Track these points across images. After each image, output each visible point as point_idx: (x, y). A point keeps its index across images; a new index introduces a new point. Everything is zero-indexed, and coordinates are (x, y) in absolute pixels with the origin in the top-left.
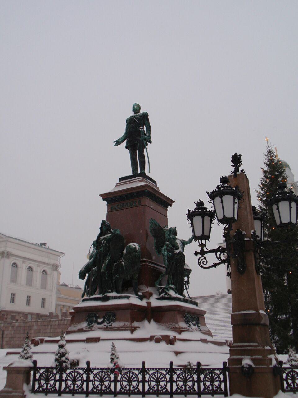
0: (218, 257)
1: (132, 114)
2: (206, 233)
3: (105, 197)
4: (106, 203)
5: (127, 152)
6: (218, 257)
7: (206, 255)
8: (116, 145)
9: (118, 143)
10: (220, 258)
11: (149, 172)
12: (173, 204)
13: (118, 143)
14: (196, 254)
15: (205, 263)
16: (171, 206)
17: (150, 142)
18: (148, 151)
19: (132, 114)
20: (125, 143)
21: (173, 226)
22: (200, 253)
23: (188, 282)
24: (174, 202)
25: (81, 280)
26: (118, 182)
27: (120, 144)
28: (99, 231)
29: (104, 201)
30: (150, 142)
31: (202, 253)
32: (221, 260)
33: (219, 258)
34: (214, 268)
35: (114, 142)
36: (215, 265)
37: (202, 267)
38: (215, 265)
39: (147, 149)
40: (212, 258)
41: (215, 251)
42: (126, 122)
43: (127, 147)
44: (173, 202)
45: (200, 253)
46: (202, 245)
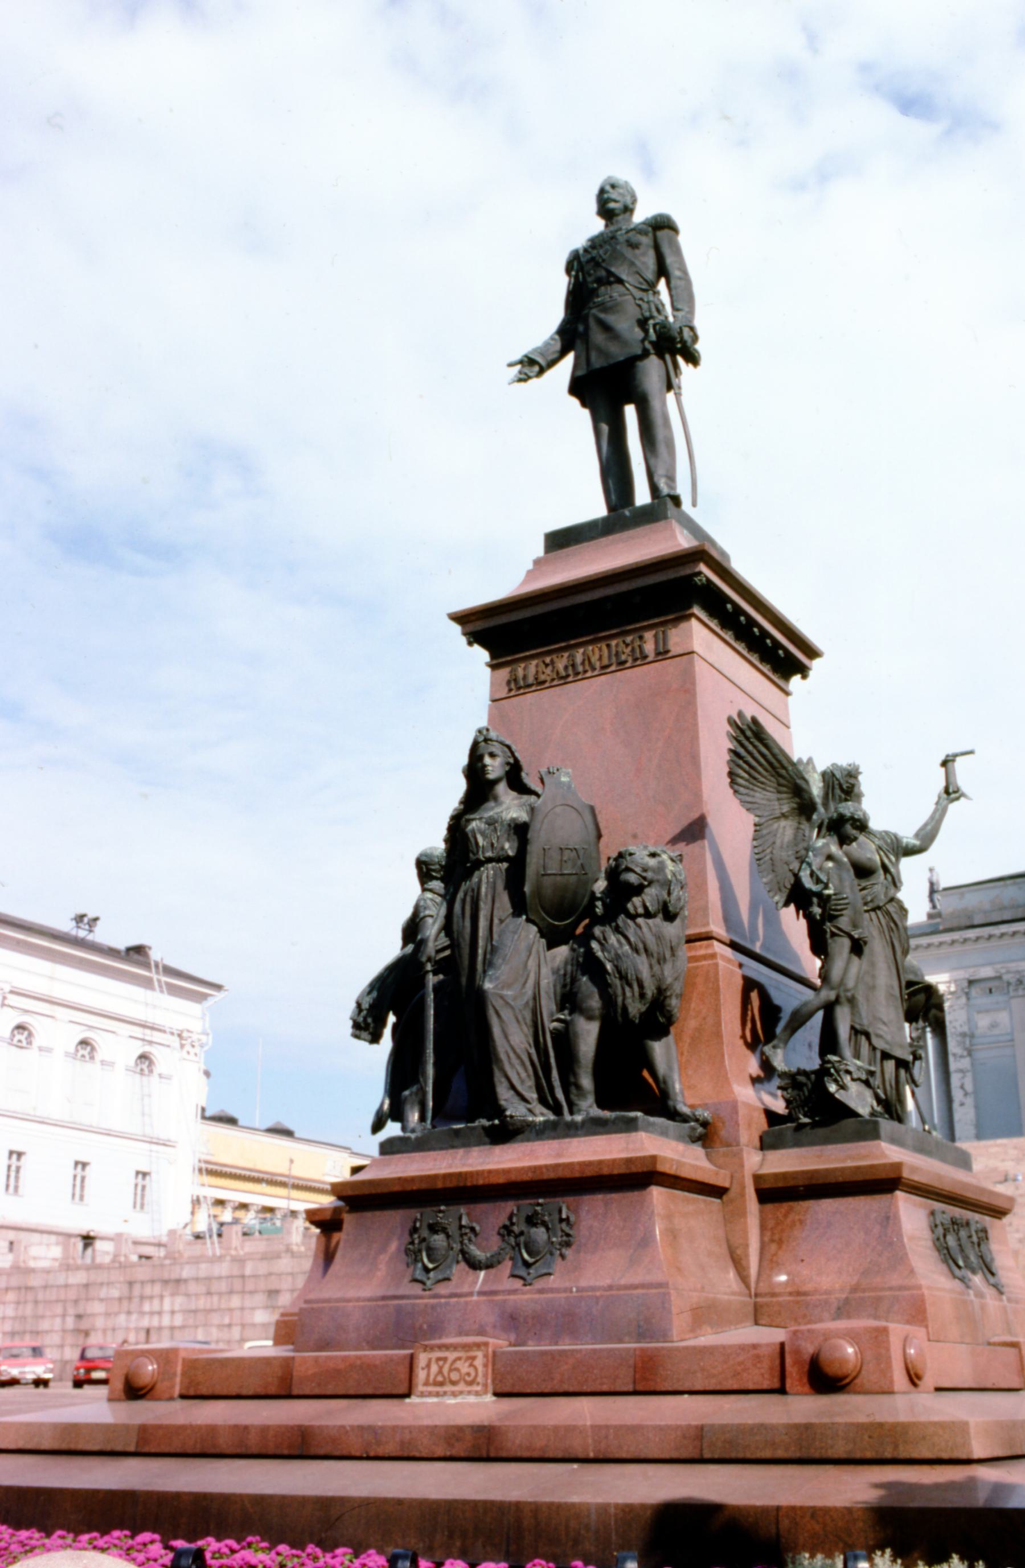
1: (598, 226)
4: (481, 655)
5: (578, 420)
8: (523, 378)
13: (532, 366)
16: (804, 677)
18: (684, 399)
25: (363, 1046)
26: (530, 566)
28: (460, 786)
35: (510, 365)
39: (678, 396)
42: (569, 270)
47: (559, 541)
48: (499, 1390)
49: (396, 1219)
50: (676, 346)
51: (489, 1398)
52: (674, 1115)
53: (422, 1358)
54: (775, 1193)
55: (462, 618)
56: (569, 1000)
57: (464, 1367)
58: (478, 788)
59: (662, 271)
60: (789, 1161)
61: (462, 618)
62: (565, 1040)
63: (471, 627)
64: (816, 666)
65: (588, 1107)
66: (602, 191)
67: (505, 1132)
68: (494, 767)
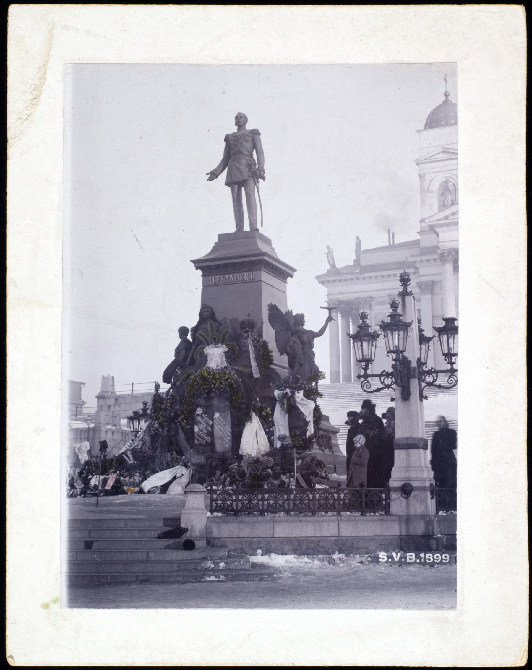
0: (382, 381)
3: (199, 264)
4: (200, 272)
6: (382, 381)
7: (369, 379)
8: (211, 179)
9: (213, 175)
10: (384, 382)
11: (262, 226)
13: (213, 175)
14: (359, 377)
15: (368, 387)
17: (264, 178)
19: (234, 129)
20: (224, 175)
21: (300, 312)
27: (217, 177)
29: (197, 269)
30: (264, 178)
31: (366, 376)
32: (385, 385)
33: (383, 383)
35: (207, 174)
36: (378, 390)
37: (365, 391)
38: (378, 390)
39: (258, 189)
41: (380, 376)
42: (225, 141)
43: (228, 183)
44: (294, 270)
50: (258, 174)
59: (255, 147)
64: (295, 274)
66: (237, 118)
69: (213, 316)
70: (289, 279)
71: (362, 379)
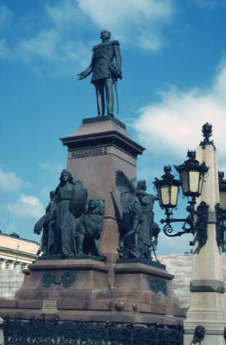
2: (173, 203)
4: (66, 147)
7: (171, 224)
12: (144, 151)
13: (83, 75)
20: (90, 77)
22: (166, 221)
23: (156, 242)
24: (144, 149)
25: (36, 235)
30: (121, 78)
31: (168, 221)
32: (185, 229)
34: (178, 237)
36: (179, 234)
38: (179, 234)
39: (116, 87)
40: (177, 227)
43: (93, 82)
44: (143, 149)
45: (166, 221)
46: (168, 214)
47: (86, 122)
48: (59, 307)
49: (42, 273)
51: (56, 310)
52: (98, 255)
53: (44, 301)
54: (118, 272)
55: (63, 140)
56: (78, 230)
57: (52, 304)
58: (63, 183)
59: (114, 55)
60: (121, 266)
61: (63, 140)
62: (77, 238)
63: (65, 142)
65: (81, 253)
67: (64, 257)
68: (66, 178)
69: (71, 180)
70: (139, 155)
71: (165, 224)
